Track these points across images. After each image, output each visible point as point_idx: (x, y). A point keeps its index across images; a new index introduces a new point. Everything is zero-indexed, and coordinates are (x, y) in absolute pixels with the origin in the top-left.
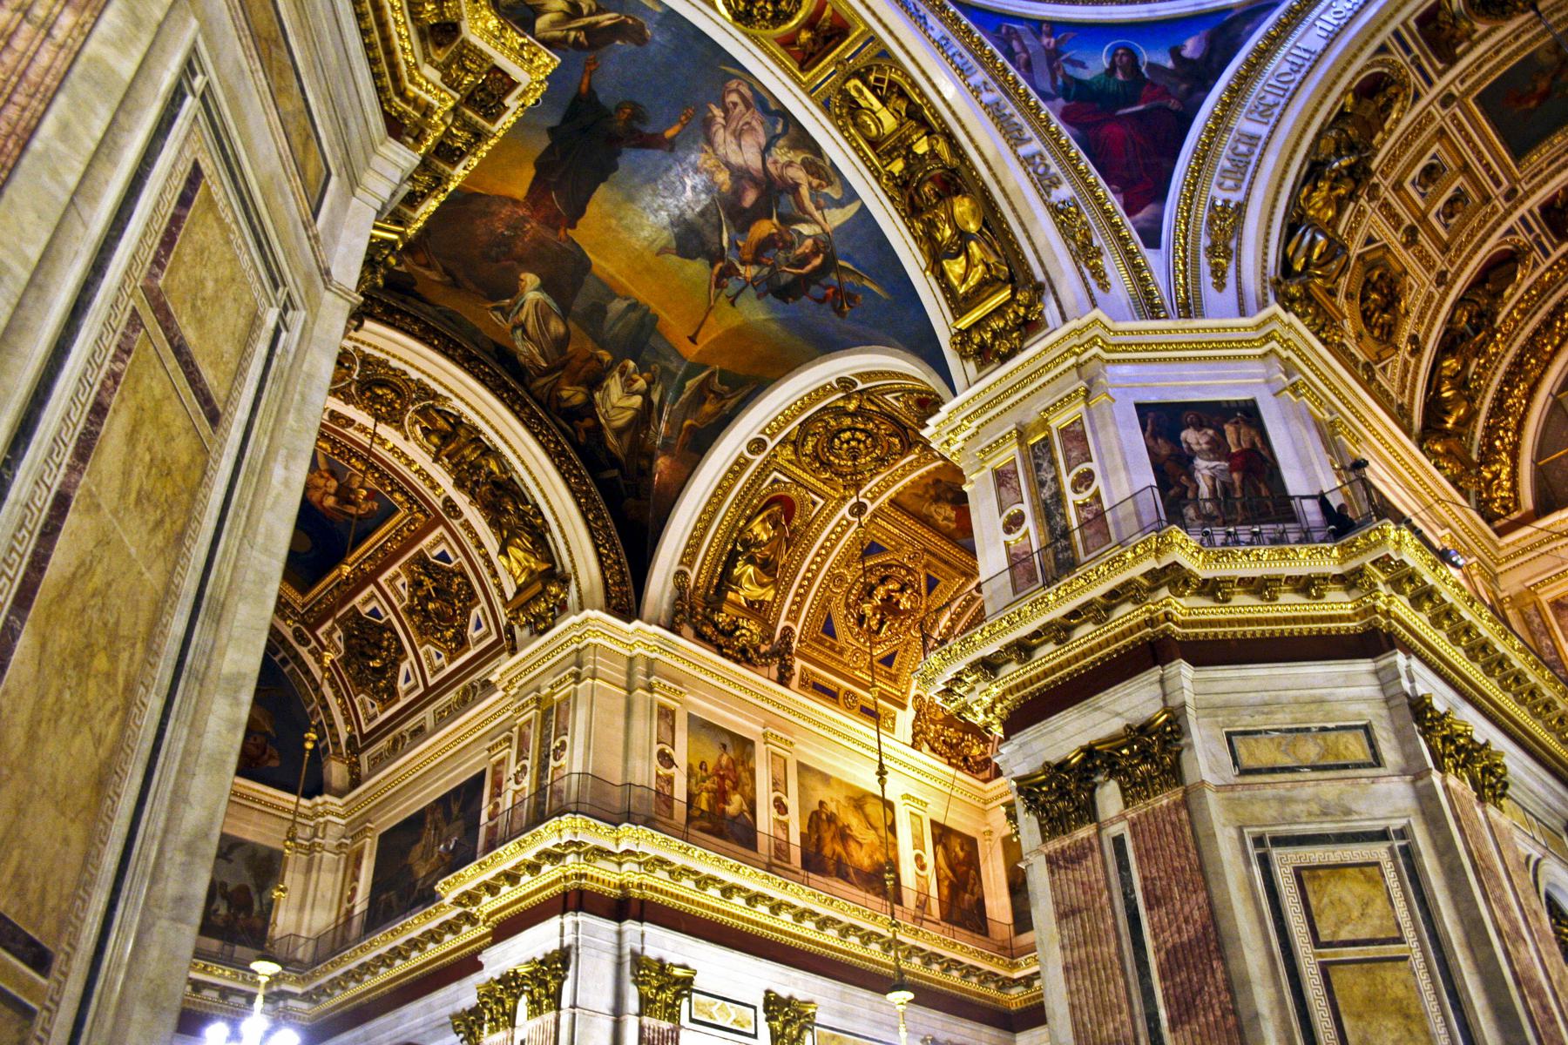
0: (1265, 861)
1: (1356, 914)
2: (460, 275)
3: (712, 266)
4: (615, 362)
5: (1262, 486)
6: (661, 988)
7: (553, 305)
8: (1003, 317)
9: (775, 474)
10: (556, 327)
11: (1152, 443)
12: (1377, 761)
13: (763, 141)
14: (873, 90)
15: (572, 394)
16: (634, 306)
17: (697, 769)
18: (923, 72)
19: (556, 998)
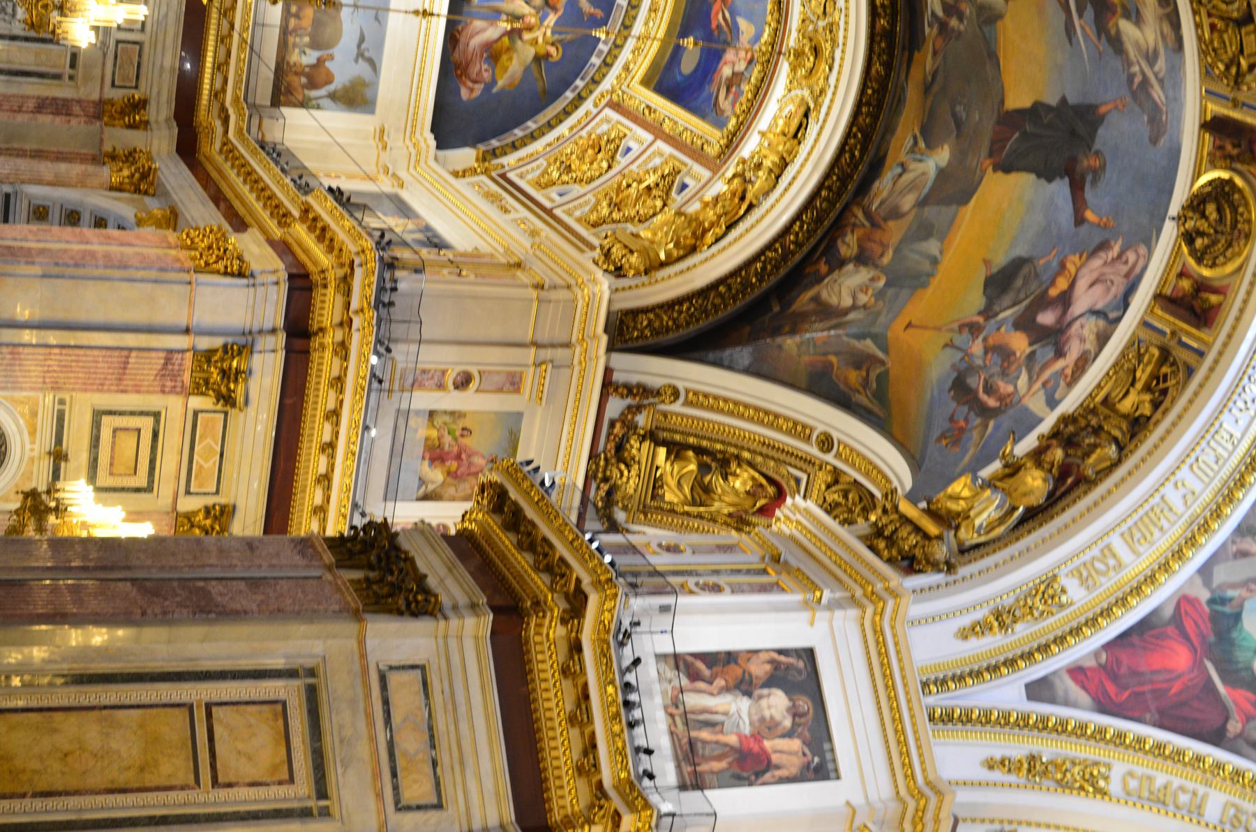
0: (291, 674)
1: (240, 746)
2: (935, 88)
3: (980, 313)
4: (884, 270)
5: (723, 765)
6: (224, 373)
7: (926, 190)
8: (909, 534)
9: (804, 477)
10: (908, 202)
11: (764, 656)
12: (400, 807)
13: (1099, 306)
14: (1155, 376)
15: (848, 245)
16: (935, 262)
17: (462, 423)
18: (1180, 417)
19: (207, 269)
